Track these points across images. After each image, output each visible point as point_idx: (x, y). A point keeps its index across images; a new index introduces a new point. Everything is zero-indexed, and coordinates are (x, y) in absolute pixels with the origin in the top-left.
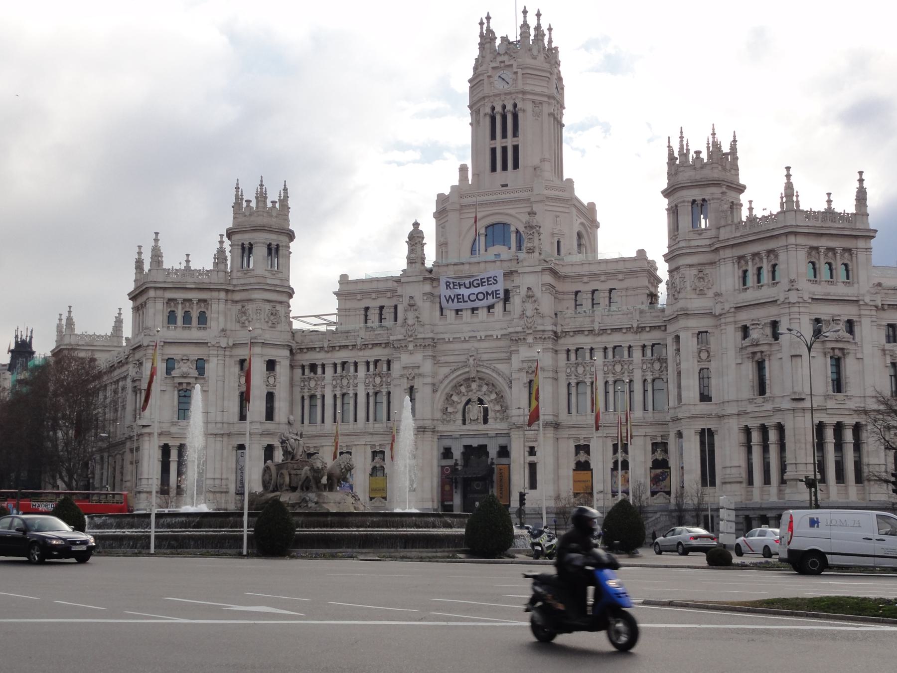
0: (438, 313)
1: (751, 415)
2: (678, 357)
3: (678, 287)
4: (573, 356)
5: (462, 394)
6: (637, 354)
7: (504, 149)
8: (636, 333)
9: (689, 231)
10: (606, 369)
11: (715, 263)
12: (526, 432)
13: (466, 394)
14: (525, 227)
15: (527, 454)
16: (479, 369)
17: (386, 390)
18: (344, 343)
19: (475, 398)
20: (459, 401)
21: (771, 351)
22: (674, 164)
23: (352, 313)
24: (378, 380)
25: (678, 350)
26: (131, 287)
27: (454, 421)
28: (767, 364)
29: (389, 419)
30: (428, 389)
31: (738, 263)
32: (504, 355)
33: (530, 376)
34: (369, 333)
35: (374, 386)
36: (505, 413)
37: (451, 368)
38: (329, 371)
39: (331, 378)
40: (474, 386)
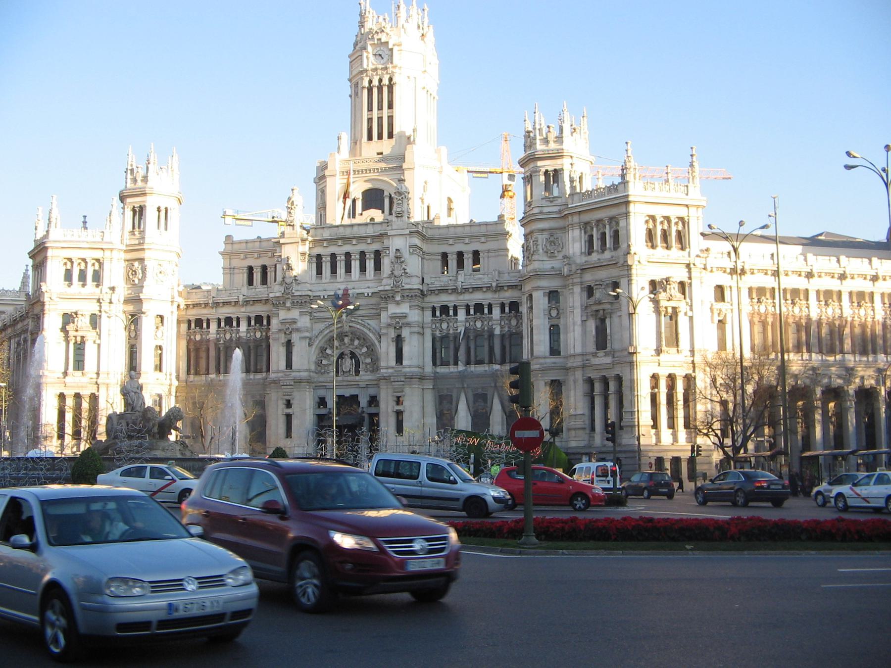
0: (314, 272)
1: (594, 367)
2: (531, 314)
3: (532, 249)
6: (496, 312)
7: (380, 119)
8: (495, 291)
9: (542, 199)
10: (468, 325)
11: (565, 228)
12: (393, 383)
14: (395, 193)
15: (395, 403)
16: (351, 324)
18: (227, 299)
19: (347, 352)
21: (612, 309)
22: (529, 137)
23: (235, 271)
25: (531, 308)
26: (32, 246)
27: (328, 373)
28: (608, 321)
29: (268, 370)
31: (585, 229)
32: (374, 311)
33: (396, 331)
34: (250, 290)
36: (375, 366)
37: (326, 323)
38: (214, 326)
39: (215, 332)
40: (346, 340)
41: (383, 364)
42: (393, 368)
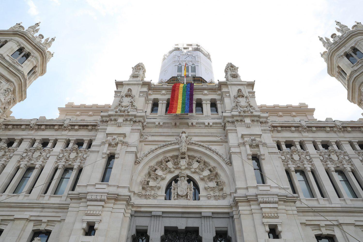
4: (284, 147)
5: (168, 170)
12: (262, 205)
13: (172, 170)
16: (190, 147)
17: (79, 164)
20: (164, 176)
27: (155, 197)
30: (131, 158)
33: (253, 150)
35: (67, 160)
36: (221, 194)
40: (183, 163)
41: (240, 184)
42: (257, 187)
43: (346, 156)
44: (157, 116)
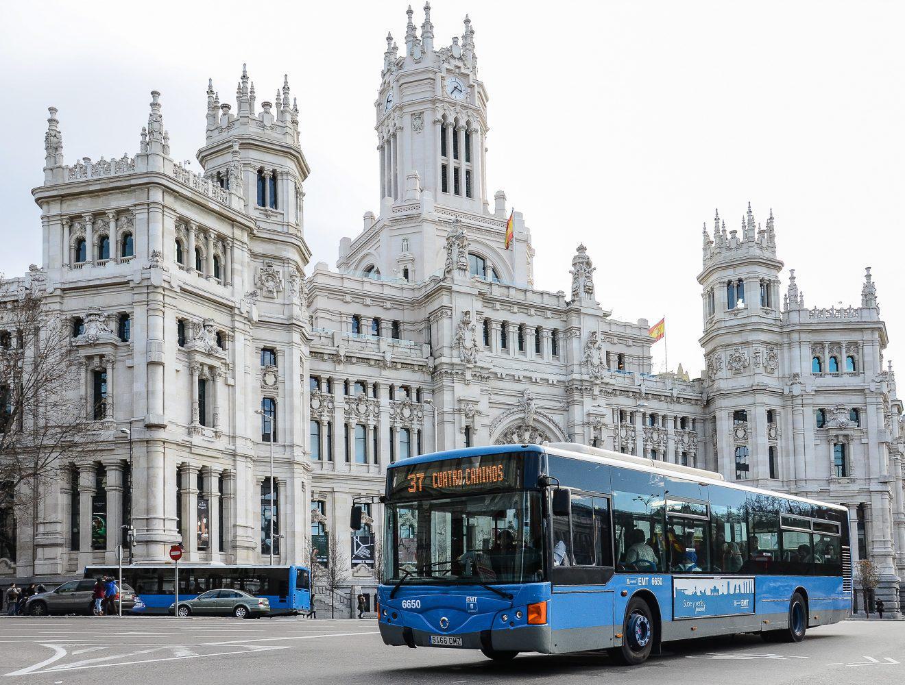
8: (672, 401)
16: (535, 416)
24: (407, 412)
32: (558, 405)
37: (502, 411)
38: (339, 389)
40: (527, 435)
43: (665, 435)
44: (493, 354)
